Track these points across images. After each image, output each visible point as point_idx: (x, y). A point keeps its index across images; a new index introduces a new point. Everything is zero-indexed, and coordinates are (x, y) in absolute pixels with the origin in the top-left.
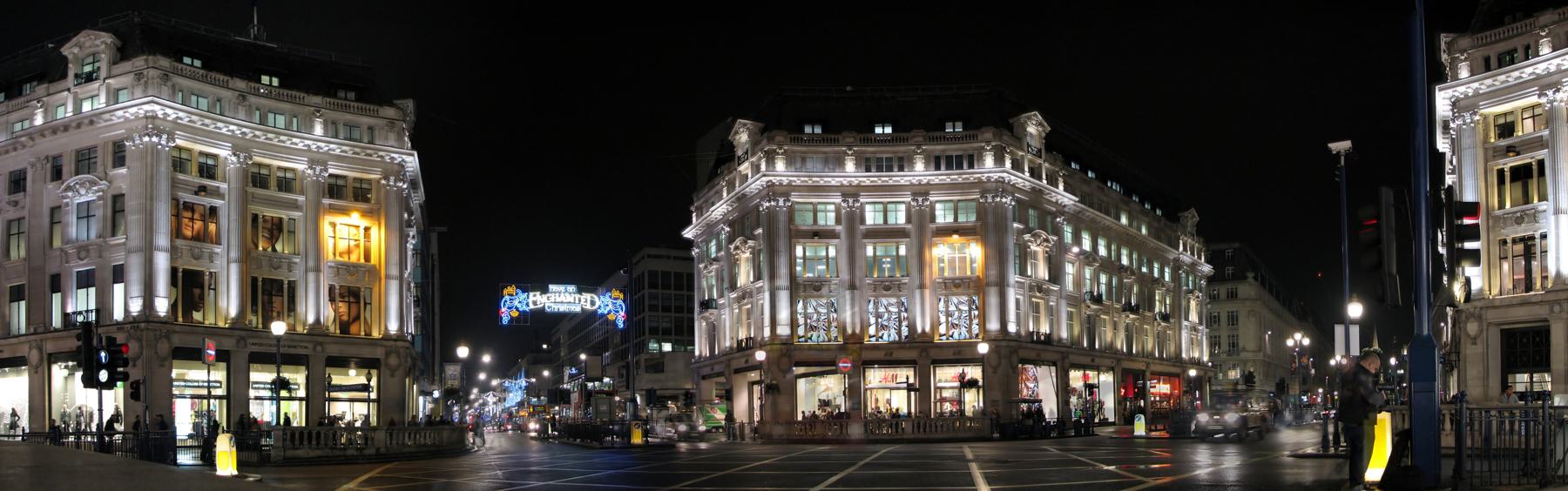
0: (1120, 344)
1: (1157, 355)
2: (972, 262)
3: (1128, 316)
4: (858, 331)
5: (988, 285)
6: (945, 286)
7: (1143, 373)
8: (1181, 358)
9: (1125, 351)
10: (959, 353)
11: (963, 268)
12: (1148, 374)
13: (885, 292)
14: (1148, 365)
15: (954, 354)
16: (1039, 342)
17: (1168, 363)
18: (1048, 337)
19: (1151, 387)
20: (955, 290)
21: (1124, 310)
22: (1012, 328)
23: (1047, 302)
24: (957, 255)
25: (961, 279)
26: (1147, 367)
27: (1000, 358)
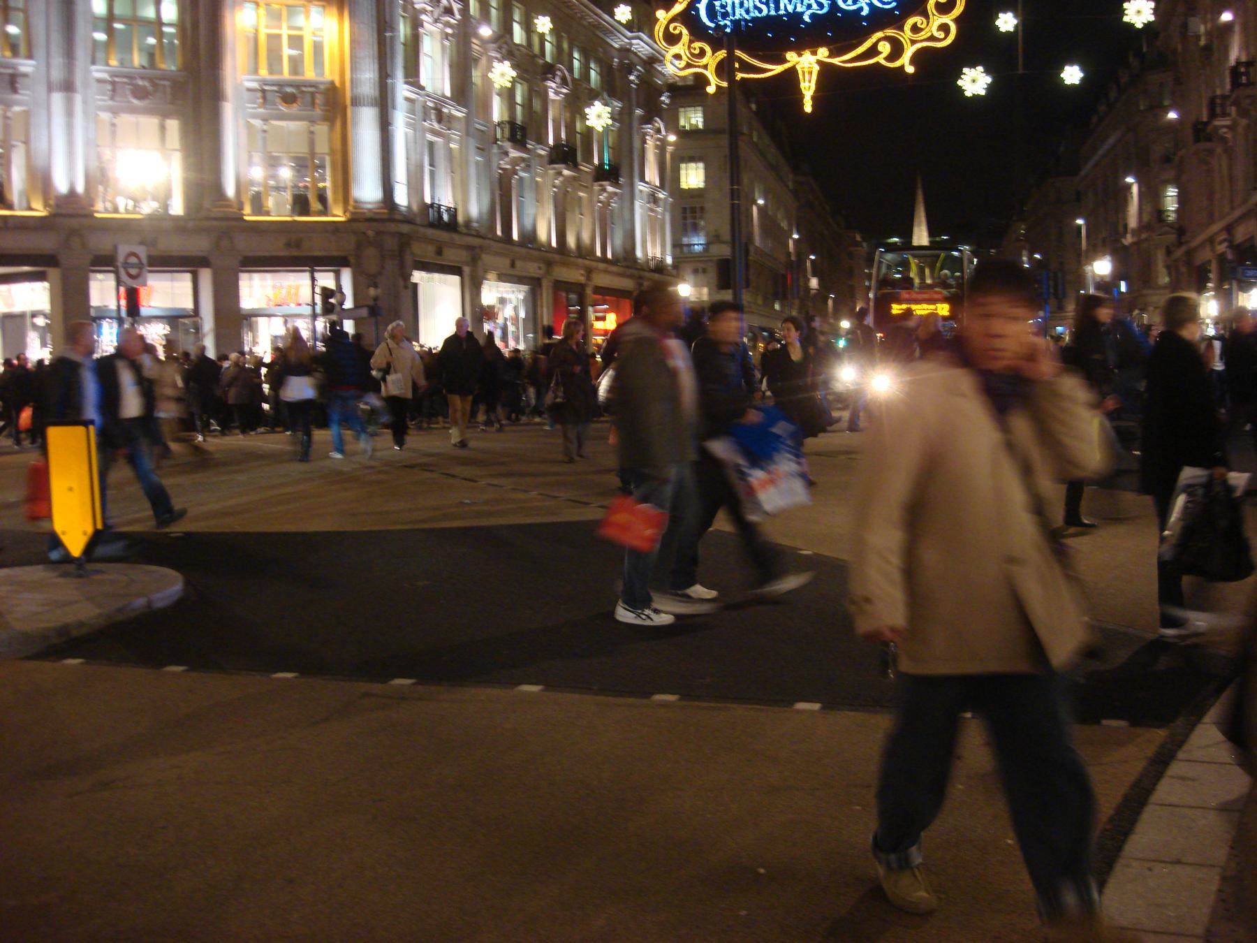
0: (546, 231)
1: (599, 254)
2: (318, 48)
3: (560, 174)
4: (80, 188)
5: (356, 102)
6: (264, 98)
7: (579, 289)
8: (635, 259)
9: (554, 244)
10: (298, 245)
11: (296, 64)
12: (589, 291)
13: (135, 102)
14: (589, 272)
15: (288, 245)
16: (438, 224)
17: (614, 269)
18: (453, 213)
19: (598, 319)
20: (283, 108)
21: (552, 161)
22: (401, 197)
23: (448, 140)
24: (285, 32)
25: (297, 85)
26: (589, 278)
27: (383, 257)
